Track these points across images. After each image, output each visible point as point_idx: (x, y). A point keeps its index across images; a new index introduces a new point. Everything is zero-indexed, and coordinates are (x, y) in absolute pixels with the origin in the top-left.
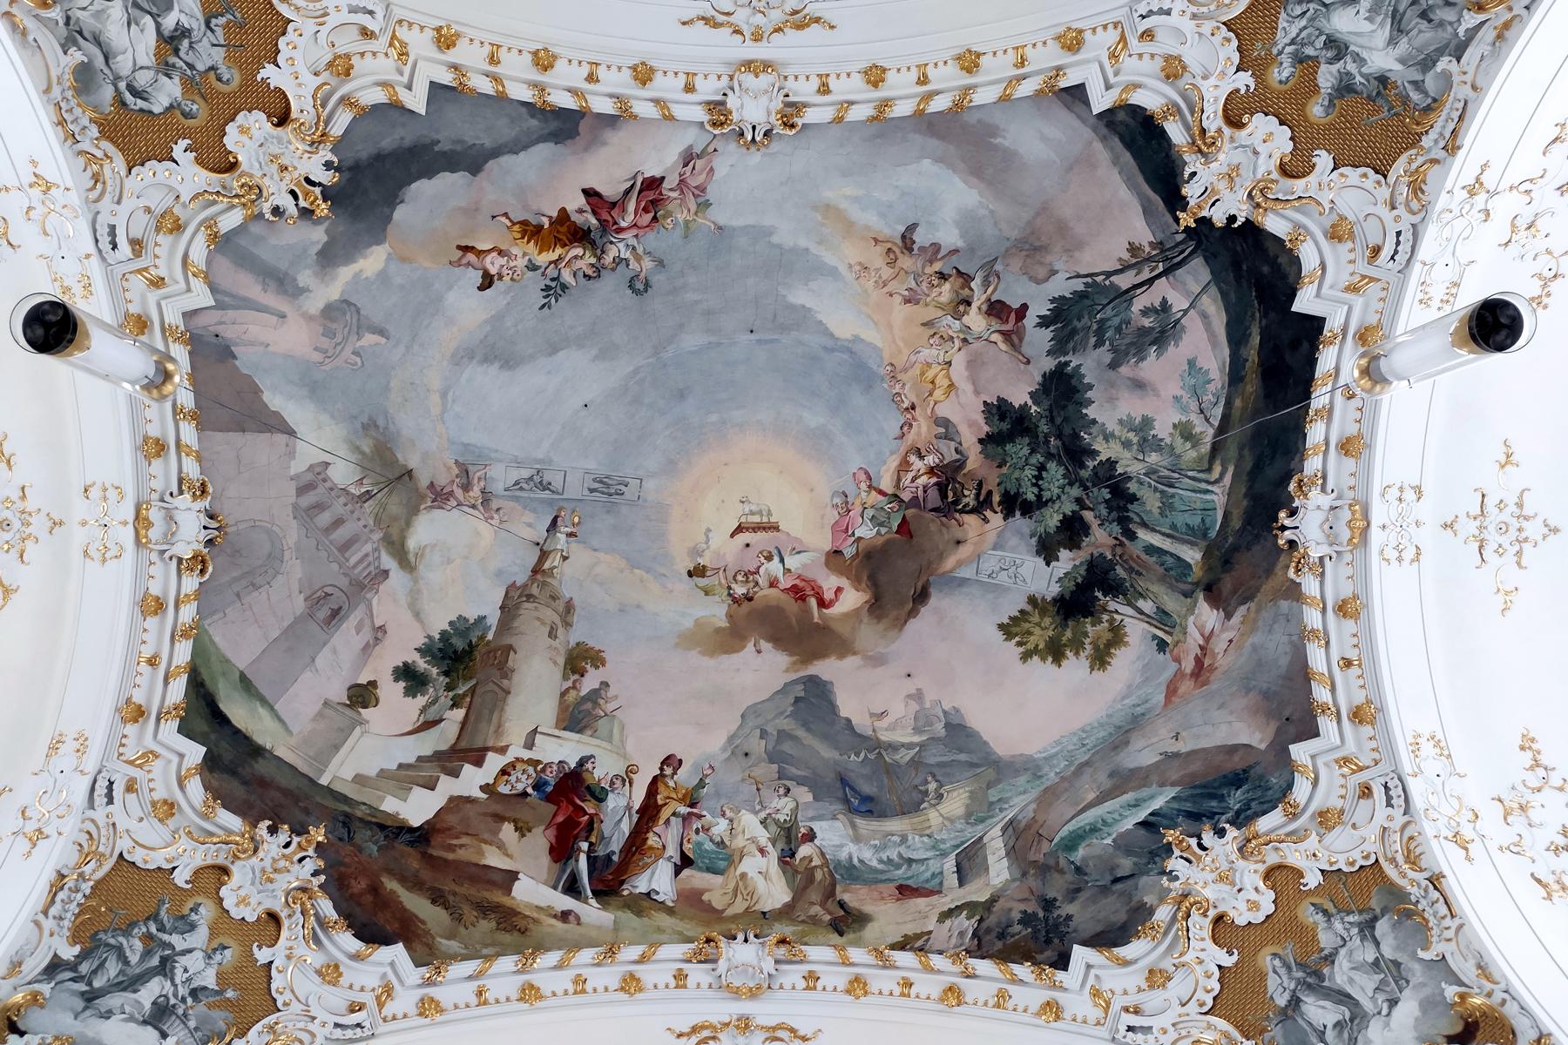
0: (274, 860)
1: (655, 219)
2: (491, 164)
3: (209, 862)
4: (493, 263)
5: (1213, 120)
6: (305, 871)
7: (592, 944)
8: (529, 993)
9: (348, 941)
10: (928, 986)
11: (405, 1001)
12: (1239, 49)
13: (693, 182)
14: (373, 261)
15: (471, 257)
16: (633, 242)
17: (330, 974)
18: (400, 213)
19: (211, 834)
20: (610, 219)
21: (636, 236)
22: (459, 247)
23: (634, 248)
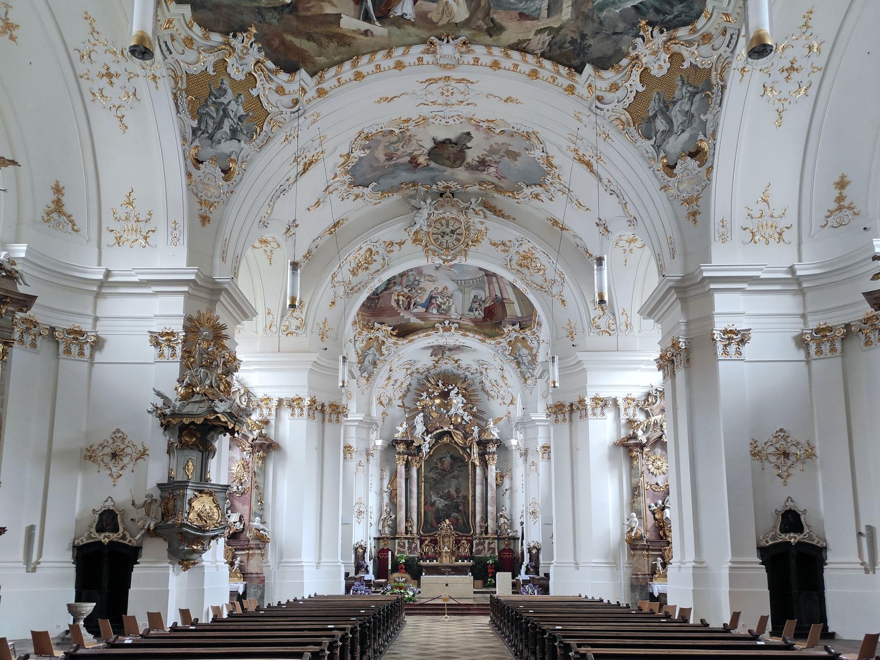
0: (242, 51)
3: (217, 59)
6: (255, 54)
7: (382, 49)
8: (359, 76)
9: (283, 76)
10: (525, 68)
11: (311, 93)
17: (280, 91)
19: (213, 47)
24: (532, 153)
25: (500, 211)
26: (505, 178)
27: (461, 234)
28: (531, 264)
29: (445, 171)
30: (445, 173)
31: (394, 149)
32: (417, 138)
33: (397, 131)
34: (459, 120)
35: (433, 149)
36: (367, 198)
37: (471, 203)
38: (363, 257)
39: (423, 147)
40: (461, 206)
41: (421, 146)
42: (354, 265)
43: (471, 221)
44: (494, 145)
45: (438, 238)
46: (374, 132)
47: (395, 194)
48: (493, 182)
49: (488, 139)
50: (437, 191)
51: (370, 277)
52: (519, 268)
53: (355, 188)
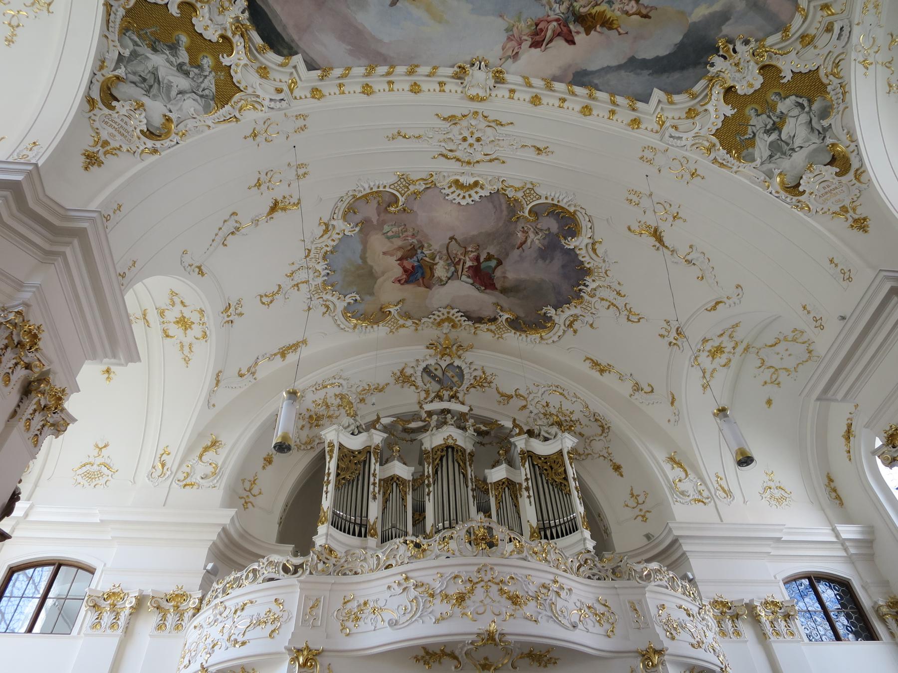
1: (537, 25)
2: (623, 62)
4: (633, 7)
5: (237, 40)
12: (232, 77)
13: (514, 43)
14: (700, 13)
15: (644, 11)
16: (550, 13)
18: (678, 38)
20: (562, 27)
21: (548, 16)
22: (650, 17)
23: (551, 9)
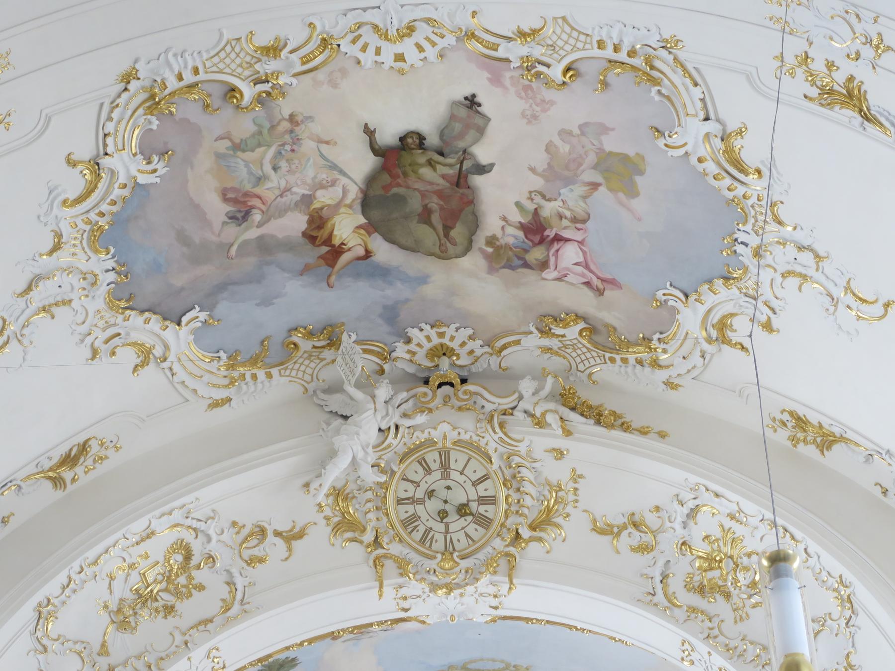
24: (676, 140)
25: (613, 413)
26: (612, 283)
27: (491, 500)
28: (736, 581)
29: (423, 280)
30: (429, 290)
31: (250, 173)
32: (315, 128)
33: (248, 92)
34: (434, 44)
35: (371, 180)
36: (181, 375)
37: (521, 398)
38: (159, 569)
39: (344, 174)
40: (489, 407)
41: (334, 167)
42: (122, 590)
43: (522, 448)
44: (557, 141)
45: (415, 518)
46: (173, 84)
47: (275, 371)
48: (581, 310)
49: (535, 117)
50: (411, 369)
51: (179, 639)
52: (695, 600)
53: (136, 319)
